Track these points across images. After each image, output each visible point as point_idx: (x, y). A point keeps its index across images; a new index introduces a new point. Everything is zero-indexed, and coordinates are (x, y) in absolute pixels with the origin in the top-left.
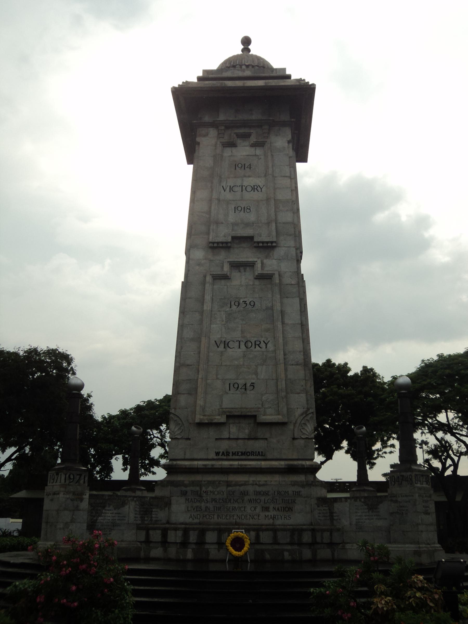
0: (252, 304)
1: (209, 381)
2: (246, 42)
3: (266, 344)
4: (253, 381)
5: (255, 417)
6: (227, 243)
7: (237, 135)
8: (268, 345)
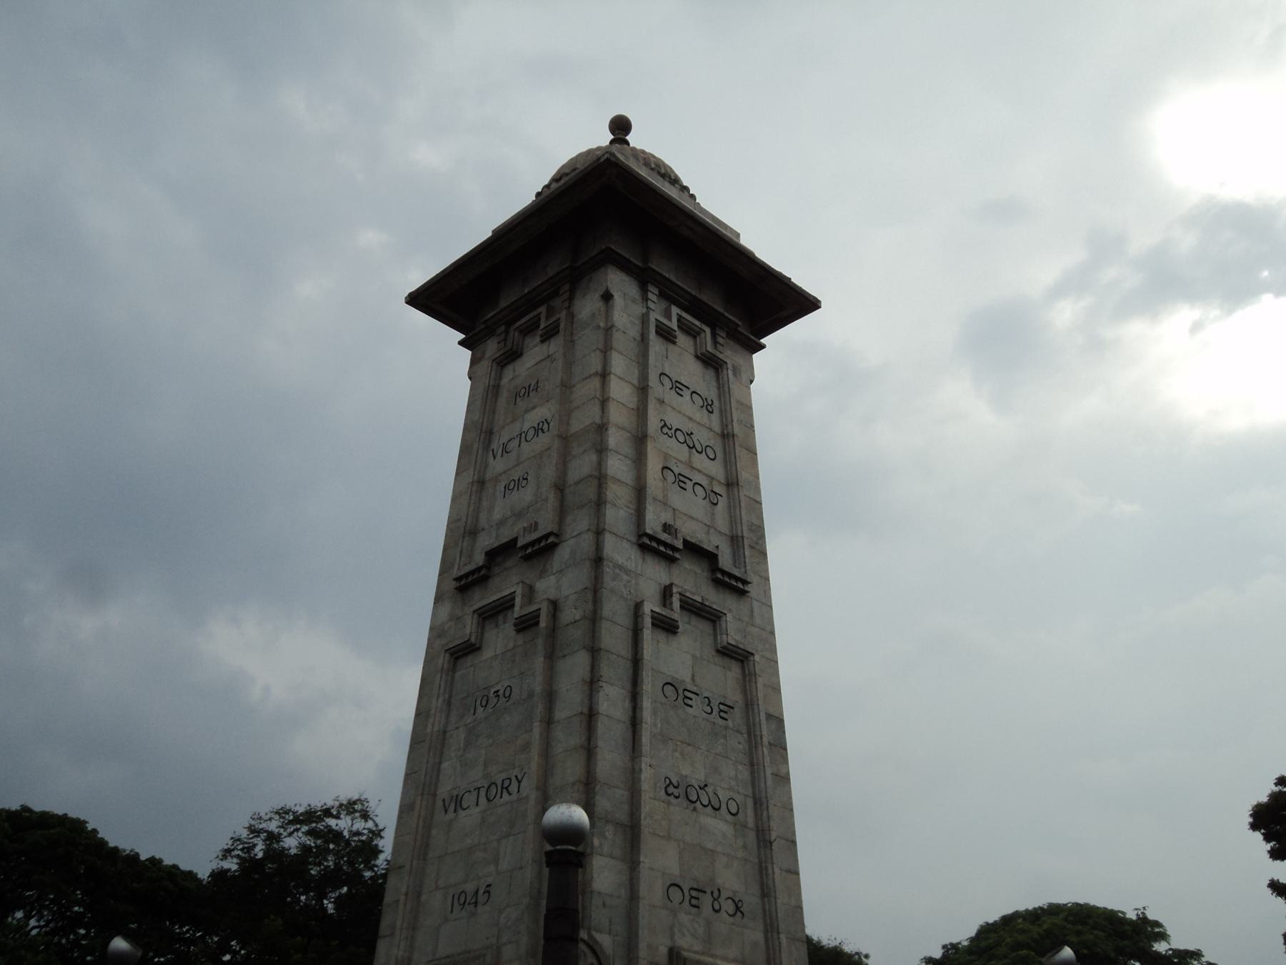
0: (507, 694)
1: (424, 897)
2: (620, 126)
3: (520, 782)
4: (490, 880)
6: (478, 569)
7: (521, 332)
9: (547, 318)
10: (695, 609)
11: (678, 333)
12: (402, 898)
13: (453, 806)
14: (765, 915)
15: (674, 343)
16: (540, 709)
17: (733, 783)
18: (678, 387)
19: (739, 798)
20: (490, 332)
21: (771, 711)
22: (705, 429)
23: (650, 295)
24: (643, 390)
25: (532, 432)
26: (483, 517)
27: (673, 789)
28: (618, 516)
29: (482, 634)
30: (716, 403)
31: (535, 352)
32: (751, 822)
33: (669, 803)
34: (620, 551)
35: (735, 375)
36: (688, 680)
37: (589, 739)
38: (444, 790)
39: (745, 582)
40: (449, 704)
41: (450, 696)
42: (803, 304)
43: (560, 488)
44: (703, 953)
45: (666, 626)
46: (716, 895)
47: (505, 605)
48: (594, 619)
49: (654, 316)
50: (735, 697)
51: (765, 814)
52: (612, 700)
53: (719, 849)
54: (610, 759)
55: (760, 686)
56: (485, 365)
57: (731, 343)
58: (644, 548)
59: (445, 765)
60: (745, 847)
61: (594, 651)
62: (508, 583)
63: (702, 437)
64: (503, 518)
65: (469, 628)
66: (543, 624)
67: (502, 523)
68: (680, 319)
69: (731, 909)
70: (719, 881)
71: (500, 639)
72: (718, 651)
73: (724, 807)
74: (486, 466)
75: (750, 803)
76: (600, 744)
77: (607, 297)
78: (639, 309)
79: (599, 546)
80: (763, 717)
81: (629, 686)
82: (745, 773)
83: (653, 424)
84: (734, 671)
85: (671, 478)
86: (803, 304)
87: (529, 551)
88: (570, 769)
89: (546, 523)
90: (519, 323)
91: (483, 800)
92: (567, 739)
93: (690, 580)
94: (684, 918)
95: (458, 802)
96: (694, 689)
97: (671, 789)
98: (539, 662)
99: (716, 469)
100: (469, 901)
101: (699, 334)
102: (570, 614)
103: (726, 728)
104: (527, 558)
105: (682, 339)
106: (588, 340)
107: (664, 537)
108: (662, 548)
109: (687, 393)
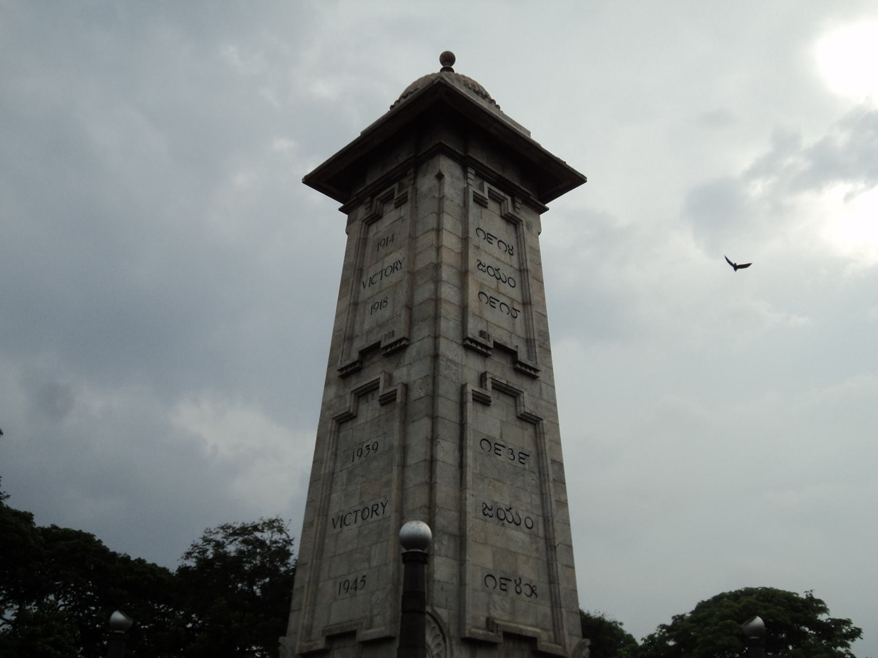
0: (375, 447)
1: (321, 585)
2: (448, 59)
3: (384, 507)
4: (365, 573)
5: (352, 634)
6: (354, 364)
7: (381, 201)
8: (386, 508)
9: (399, 191)
10: (502, 389)
11: (489, 201)
12: (306, 585)
13: (339, 523)
14: (551, 595)
15: (486, 207)
16: (397, 457)
17: (529, 507)
18: (489, 237)
19: (533, 517)
20: (359, 202)
21: (555, 458)
22: (508, 266)
23: (470, 175)
24: (465, 240)
25: (389, 270)
26: (357, 328)
27: (488, 511)
28: (449, 325)
29: (358, 407)
30: (515, 248)
31: (391, 215)
32: (541, 533)
33: (485, 521)
34: (450, 350)
35: (528, 229)
36: (498, 437)
37: (431, 477)
38: (334, 512)
39: (536, 370)
40: (336, 455)
41: (337, 449)
42: (574, 180)
43: (409, 307)
44: (509, 621)
45: (483, 401)
46: (518, 582)
47: (373, 387)
48: (433, 396)
49: (471, 189)
50: (530, 448)
51: (551, 528)
52: (446, 451)
53: (520, 551)
54: (445, 491)
55: (547, 441)
56: (357, 224)
57: (524, 206)
58: (466, 347)
59: (334, 496)
60: (537, 550)
61: (434, 418)
62: (375, 372)
63: (506, 272)
64: (371, 328)
65: (348, 403)
66: (398, 400)
67: (370, 332)
68: (490, 190)
69: (529, 592)
70: (520, 573)
71: (370, 410)
72: (518, 417)
73: (523, 523)
74: (359, 292)
75: (541, 520)
76: (438, 481)
77: (440, 177)
78: (462, 185)
79: (436, 347)
80: (549, 462)
81: (457, 441)
82: (537, 500)
83: (472, 263)
84: (529, 430)
85: (485, 299)
86: (574, 180)
87: (389, 350)
88: (418, 498)
89: (400, 331)
90: (379, 196)
91: (359, 518)
92: (416, 477)
93: (499, 369)
94: (496, 598)
95: (343, 521)
96: (502, 443)
97: (487, 511)
98: (396, 425)
99: (515, 293)
100: (351, 587)
101: (503, 201)
102: (417, 392)
103: (524, 469)
104: (387, 355)
105: (492, 205)
106: (427, 207)
107: (481, 340)
108: (479, 348)
109: (495, 242)
